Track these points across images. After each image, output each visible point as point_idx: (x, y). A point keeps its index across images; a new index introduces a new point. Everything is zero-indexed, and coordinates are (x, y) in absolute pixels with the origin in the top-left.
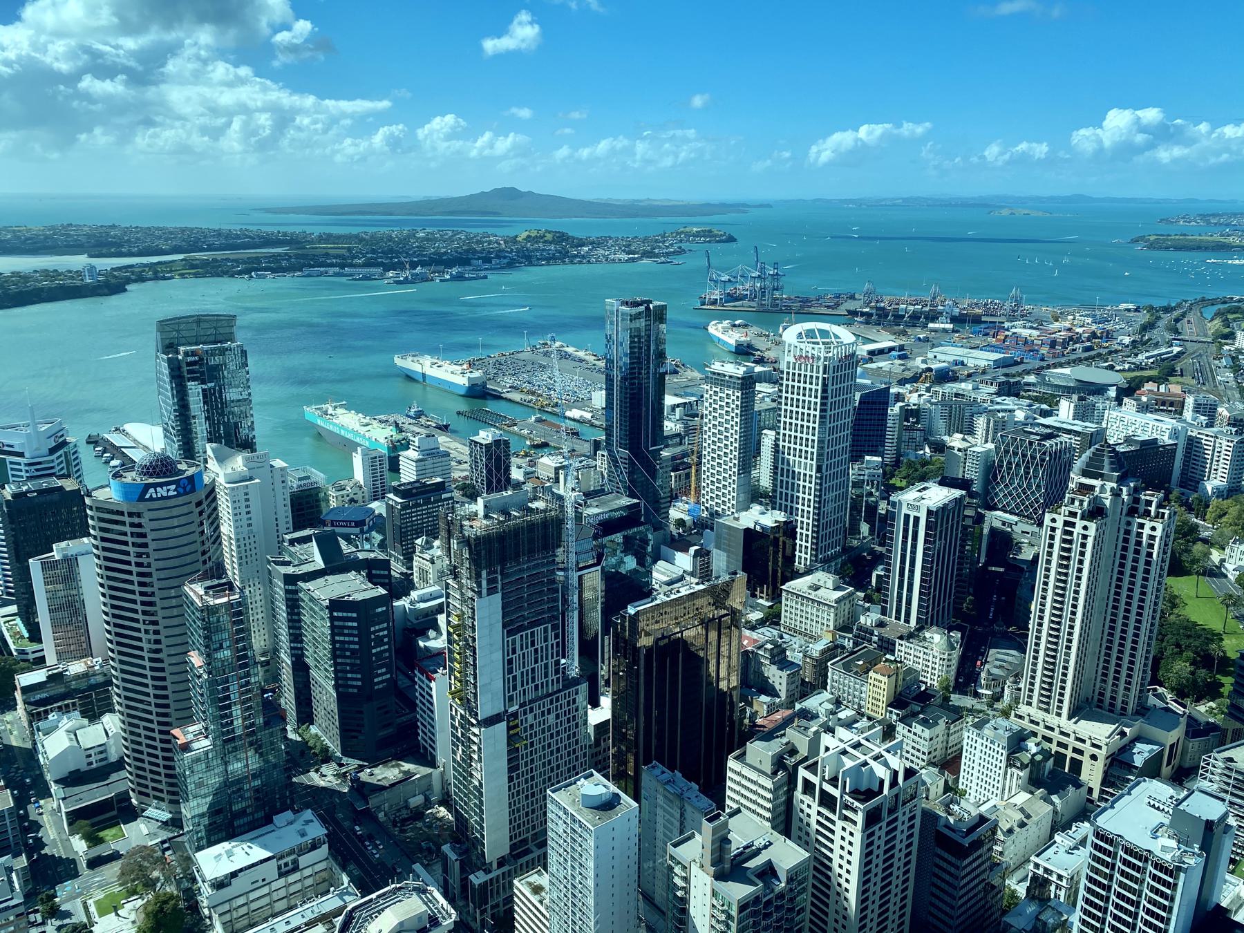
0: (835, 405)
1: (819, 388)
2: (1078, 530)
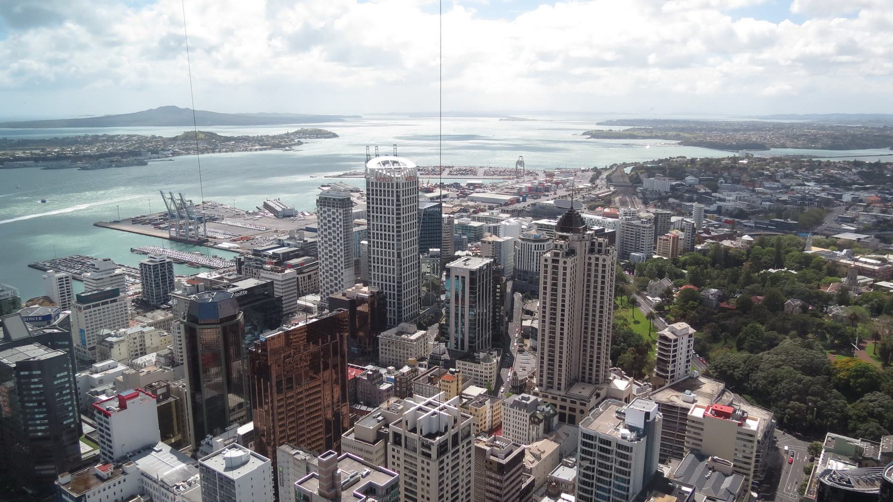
0: (406, 210)
1: (395, 198)
2: (561, 265)
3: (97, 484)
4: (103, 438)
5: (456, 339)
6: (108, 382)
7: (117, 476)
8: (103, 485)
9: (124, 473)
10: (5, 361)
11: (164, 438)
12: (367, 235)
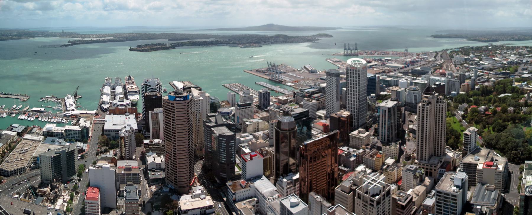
5: (382, 135)
6: (246, 142)
12: (345, 85)
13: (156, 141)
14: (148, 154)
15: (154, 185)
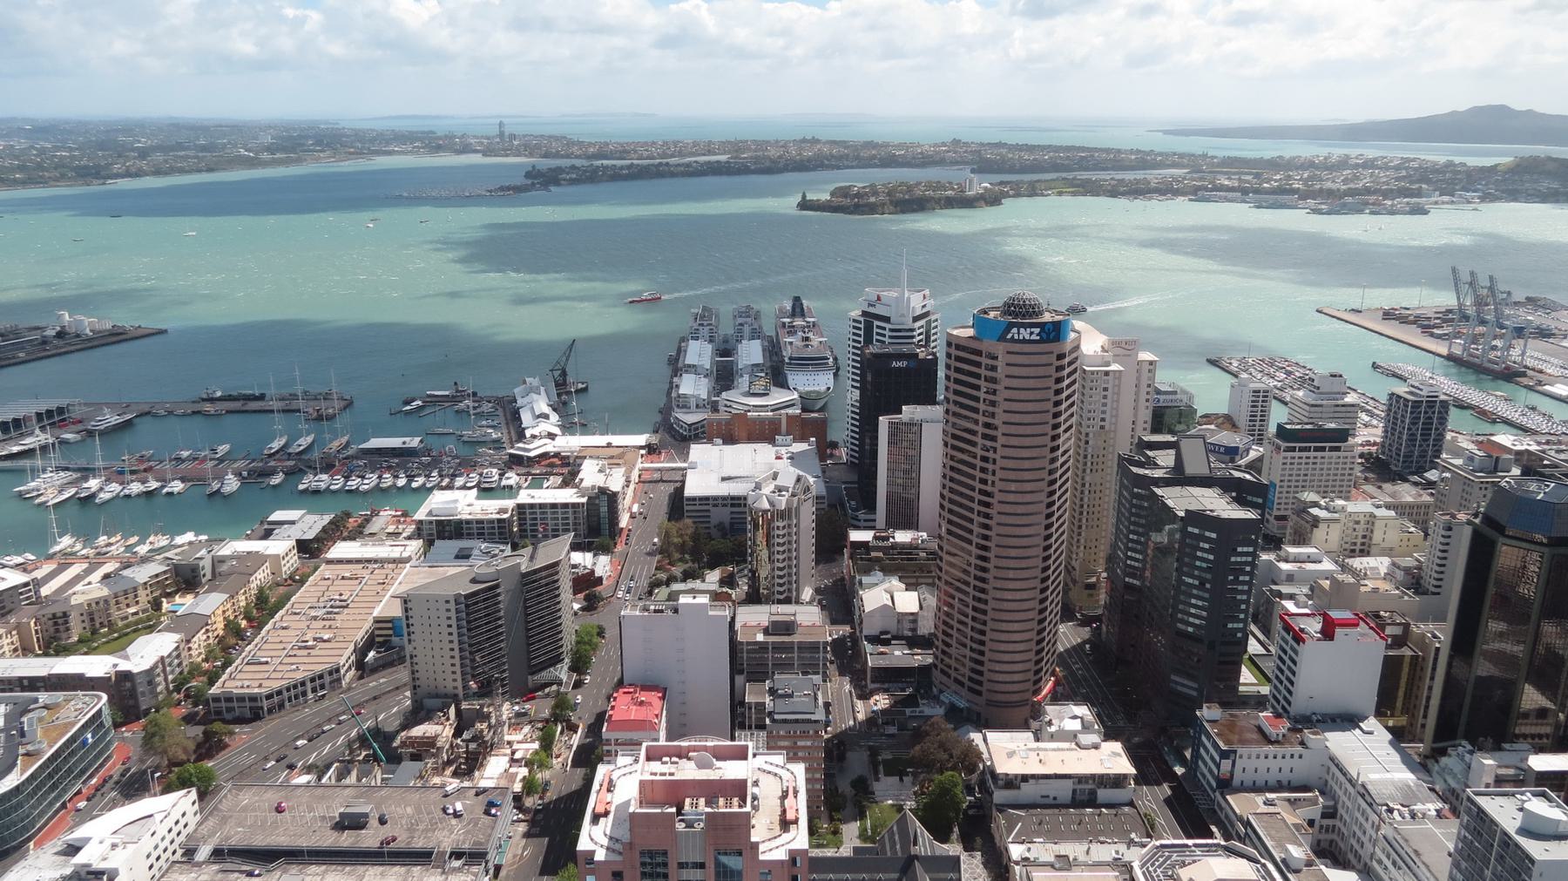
3: (1257, 742)
4: (1284, 674)
6: (1302, 582)
7: (1291, 743)
8: (1270, 749)
9: (1302, 743)
10: (1170, 503)
11: (1379, 714)
13: (902, 537)
14: (865, 580)
15: (886, 691)
